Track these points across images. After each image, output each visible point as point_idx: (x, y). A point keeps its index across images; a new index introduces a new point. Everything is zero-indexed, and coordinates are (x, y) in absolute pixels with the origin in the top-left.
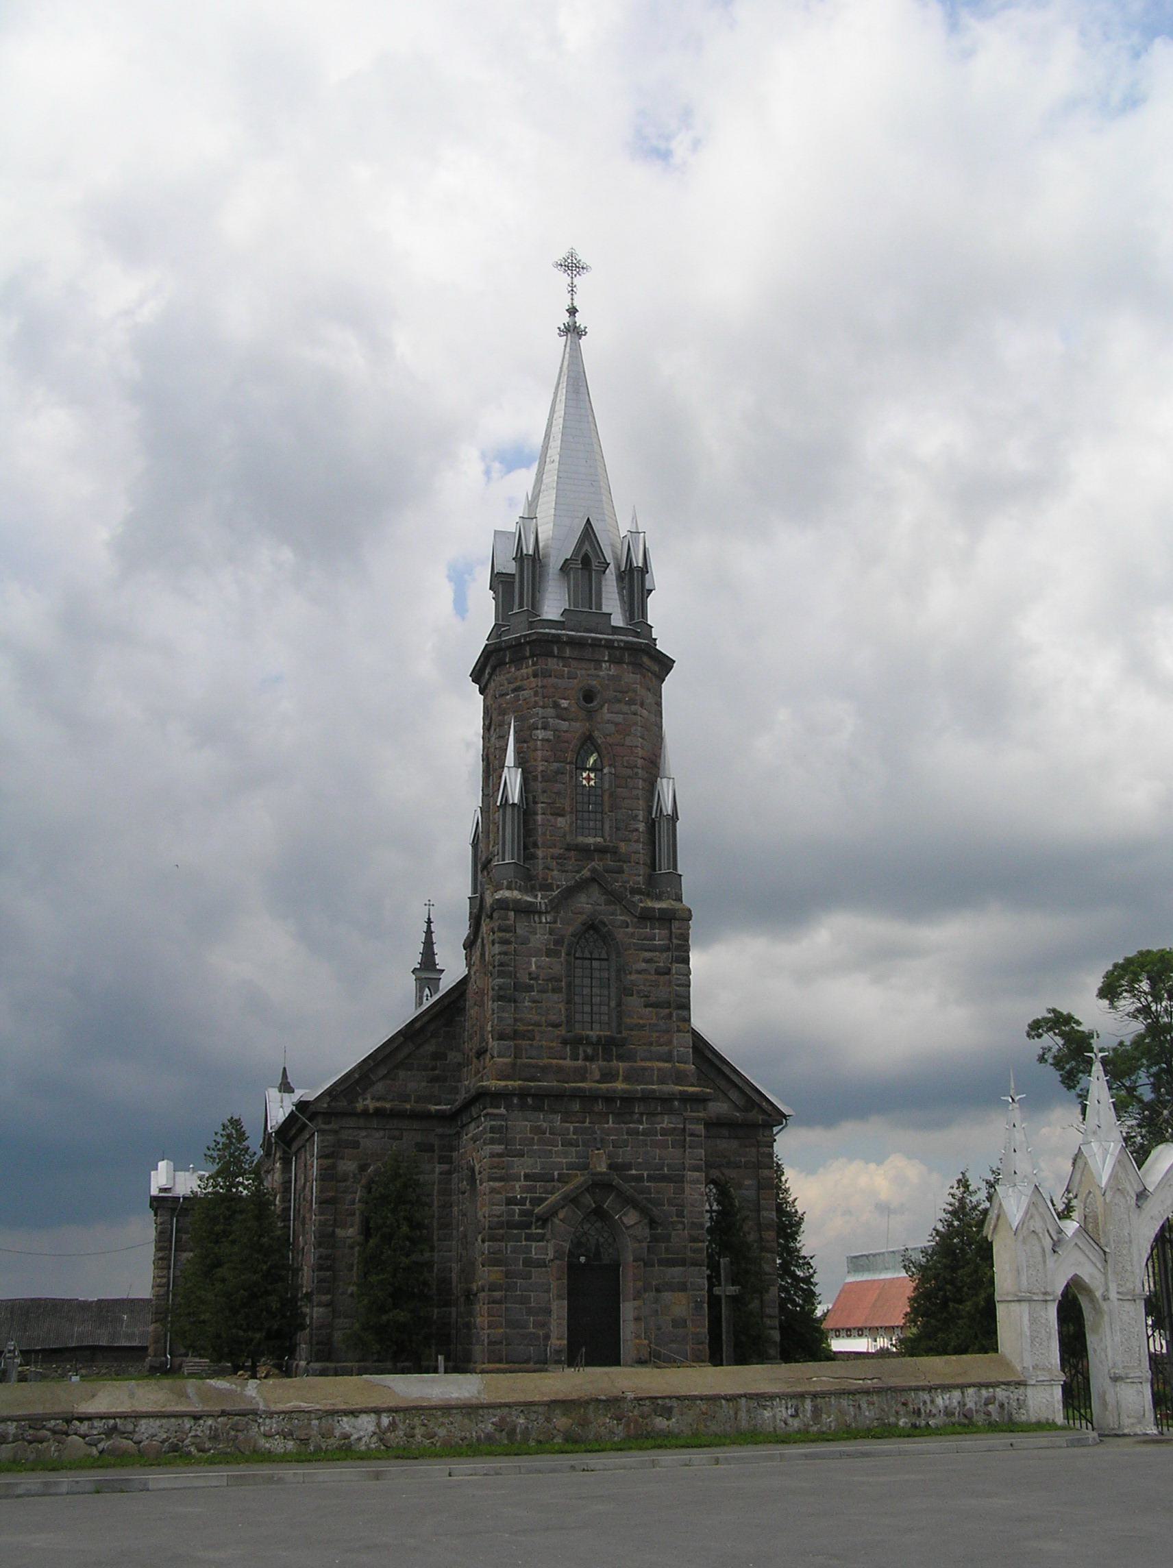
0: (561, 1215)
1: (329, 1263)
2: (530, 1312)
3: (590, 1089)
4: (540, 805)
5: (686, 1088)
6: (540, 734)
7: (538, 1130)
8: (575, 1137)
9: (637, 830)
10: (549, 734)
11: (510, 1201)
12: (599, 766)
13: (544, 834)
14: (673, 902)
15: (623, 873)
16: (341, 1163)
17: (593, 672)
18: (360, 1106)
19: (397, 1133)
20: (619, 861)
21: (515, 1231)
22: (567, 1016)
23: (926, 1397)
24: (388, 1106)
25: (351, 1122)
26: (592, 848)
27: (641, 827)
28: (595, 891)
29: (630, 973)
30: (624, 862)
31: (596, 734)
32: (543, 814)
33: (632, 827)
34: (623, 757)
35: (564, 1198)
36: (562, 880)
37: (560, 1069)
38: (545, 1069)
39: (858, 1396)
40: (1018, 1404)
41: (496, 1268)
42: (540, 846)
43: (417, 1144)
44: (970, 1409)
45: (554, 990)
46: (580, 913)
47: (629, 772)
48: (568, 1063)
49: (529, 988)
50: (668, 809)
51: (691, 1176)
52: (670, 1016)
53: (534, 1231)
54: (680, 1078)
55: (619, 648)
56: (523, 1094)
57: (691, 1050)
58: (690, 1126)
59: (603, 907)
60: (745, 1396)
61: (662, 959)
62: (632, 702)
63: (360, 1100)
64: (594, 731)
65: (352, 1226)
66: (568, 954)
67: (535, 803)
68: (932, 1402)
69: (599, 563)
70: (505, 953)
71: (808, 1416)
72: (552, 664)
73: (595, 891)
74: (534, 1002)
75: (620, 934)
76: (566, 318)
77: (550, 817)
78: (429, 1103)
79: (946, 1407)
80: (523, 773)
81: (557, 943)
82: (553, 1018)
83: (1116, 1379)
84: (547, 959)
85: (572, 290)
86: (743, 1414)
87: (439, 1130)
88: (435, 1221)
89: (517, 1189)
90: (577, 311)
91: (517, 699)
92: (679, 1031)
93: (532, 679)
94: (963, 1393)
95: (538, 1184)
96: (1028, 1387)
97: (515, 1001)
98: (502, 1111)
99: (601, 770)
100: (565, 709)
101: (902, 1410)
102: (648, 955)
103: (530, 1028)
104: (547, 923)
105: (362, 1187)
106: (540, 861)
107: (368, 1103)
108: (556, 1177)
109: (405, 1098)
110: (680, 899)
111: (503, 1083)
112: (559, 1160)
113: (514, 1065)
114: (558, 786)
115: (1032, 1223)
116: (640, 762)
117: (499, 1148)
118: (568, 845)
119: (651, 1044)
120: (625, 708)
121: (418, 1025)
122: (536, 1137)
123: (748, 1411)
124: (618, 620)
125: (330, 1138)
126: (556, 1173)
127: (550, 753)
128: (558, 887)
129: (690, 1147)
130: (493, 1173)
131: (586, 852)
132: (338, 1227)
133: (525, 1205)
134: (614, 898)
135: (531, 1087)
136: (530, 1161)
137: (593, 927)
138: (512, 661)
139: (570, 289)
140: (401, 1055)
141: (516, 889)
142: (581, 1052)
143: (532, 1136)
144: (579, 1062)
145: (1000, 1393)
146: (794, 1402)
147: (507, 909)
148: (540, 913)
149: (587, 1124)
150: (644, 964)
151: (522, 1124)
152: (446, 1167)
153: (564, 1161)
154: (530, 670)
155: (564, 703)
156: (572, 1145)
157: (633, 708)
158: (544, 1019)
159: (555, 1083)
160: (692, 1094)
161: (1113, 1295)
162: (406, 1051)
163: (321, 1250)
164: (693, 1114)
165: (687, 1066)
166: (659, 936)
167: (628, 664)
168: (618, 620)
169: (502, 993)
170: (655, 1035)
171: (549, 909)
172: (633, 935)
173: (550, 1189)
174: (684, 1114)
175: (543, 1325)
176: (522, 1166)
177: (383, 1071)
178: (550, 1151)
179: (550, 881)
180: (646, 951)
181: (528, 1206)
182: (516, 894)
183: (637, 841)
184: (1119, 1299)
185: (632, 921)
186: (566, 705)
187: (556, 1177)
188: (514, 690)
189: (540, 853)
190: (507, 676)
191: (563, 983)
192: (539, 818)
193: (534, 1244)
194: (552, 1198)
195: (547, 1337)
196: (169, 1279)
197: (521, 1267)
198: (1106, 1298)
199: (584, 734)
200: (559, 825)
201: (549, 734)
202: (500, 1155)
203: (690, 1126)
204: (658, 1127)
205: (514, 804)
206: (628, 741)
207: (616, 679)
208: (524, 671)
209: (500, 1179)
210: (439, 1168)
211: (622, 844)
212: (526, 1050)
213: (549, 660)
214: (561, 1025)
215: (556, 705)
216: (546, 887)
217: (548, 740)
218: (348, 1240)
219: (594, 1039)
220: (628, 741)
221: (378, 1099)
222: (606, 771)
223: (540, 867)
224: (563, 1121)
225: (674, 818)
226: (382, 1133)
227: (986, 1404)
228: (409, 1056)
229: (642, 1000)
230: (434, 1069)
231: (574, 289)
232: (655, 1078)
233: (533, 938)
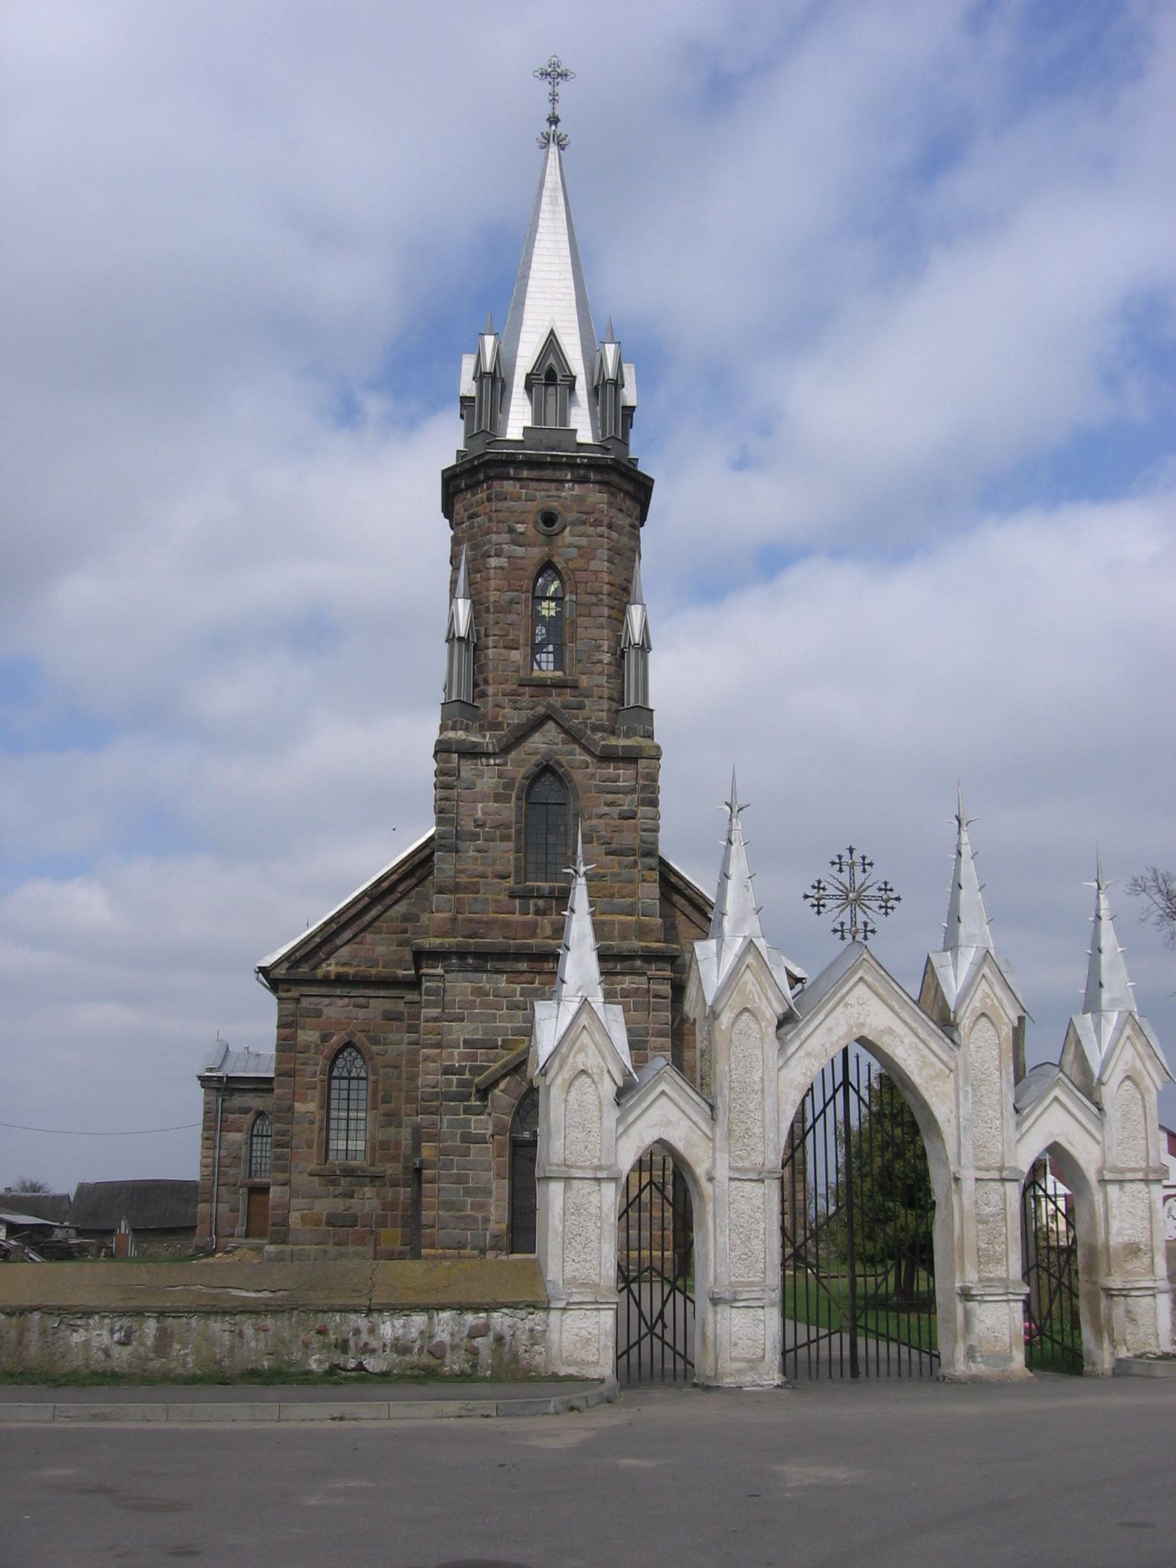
0: (502, 1085)
1: (287, 1138)
2: (468, 1192)
3: (537, 946)
4: (491, 638)
5: (649, 944)
6: (493, 562)
7: (479, 992)
8: (522, 999)
9: (600, 662)
10: (503, 561)
11: (448, 1071)
12: (560, 595)
13: (495, 668)
14: (638, 738)
15: (584, 709)
16: (300, 1032)
17: (554, 493)
18: (320, 973)
19: (363, 1001)
20: (580, 695)
21: (452, 1104)
22: (516, 867)
23: (361, 1321)
24: (351, 971)
25: (314, 990)
26: (549, 682)
27: (606, 658)
28: (551, 725)
29: (590, 818)
30: (586, 697)
31: (555, 559)
32: (494, 647)
33: (597, 657)
34: (586, 583)
35: (503, 1066)
36: (513, 717)
37: (506, 924)
38: (490, 924)
39: (238, 1318)
40: (531, 1337)
41: (429, 1144)
42: (490, 682)
44: (441, 1344)
45: (502, 839)
46: (534, 754)
47: (594, 599)
48: (517, 917)
49: (475, 837)
50: (637, 637)
51: (654, 1042)
52: (635, 864)
53: (474, 1103)
54: (643, 932)
55: (581, 466)
56: (462, 955)
57: (658, 902)
58: (654, 987)
59: (560, 746)
60: (38, 1309)
61: (628, 802)
62: (597, 523)
63: (324, 965)
64: (552, 556)
65: (313, 1100)
66: (518, 799)
67: (487, 636)
68: (372, 1330)
69: (563, 376)
70: (446, 799)
71: (149, 1343)
72: (509, 486)
73: (551, 725)
74: (479, 851)
75: (578, 776)
76: (545, 127)
77: (501, 650)
78: (399, 968)
79: (397, 1339)
80: (473, 603)
81: (508, 786)
82: (499, 868)
83: (715, 1302)
84: (496, 805)
85: (554, 99)
86: (33, 1336)
88: (403, 1094)
89: (455, 1057)
90: (559, 120)
91: (472, 527)
92: (643, 881)
93: (487, 504)
94: (431, 1318)
95: (479, 1051)
96: (552, 1313)
97: (457, 851)
98: (440, 971)
99: (562, 599)
100: (522, 533)
101: (316, 1340)
102: (610, 797)
103: (476, 879)
104: (495, 765)
106: (490, 698)
107: (331, 968)
108: (500, 1043)
109: (374, 963)
110: (650, 735)
111: (438, 941)
112: (504, 1024)
113: (454, 920)
114: (511, 618)
115: (580, 1058)
116: (606, 588)
117: (433, 1012)
118: (522, 680)
119: (612, 896)
120: (591, 530)
121: (385, 884)
122: (478, 1000)
123: (43, 1332)
124: (585, 435)
125: (292, 1006)
126: (500, 1039)
127: (503, 582)
128: (509, 725)
129: (654, 1010)
130: (428, 1039)
131: (542, 686)
132: (298, 1102)
133: (464, 1075)
134: (573, 736)
135: (469, 945)
136: (471, 1026)
137: (547, 769)
138: (468, 488)
139: (551, 98)
140: (368, 918)
141: (461, 729)
142: (531, 906)
143: (473, 998)
144: (530, 916)
145: (500, 1320)
146: (126, 1322)
147: (450, 752)
148: (488, 755)
149: (536, 985)
150: (606, 808)
151: (460, 985)
153: (509, 1025)
154: (484, 495)
155: (520, 528)
156: (518, 1008)
157: (599, 530)
158: (490, 869)
159: (501, 940)
160: (657, 950)
161: (722, 1173)
162: (373, 913)
164: (659, 973)
165: (653, 919)
166: (625, 775)
167: (595, 482)
168: (585, 435)
169: (443, 842)
170: (617, 885)
171: (497, 750)
172: (593, 775)
173: (492, 1057)
174: (649, 973)
175: (482, 1207)
176: (460, 1031)
177: (347, 934)
178: (494, 1015)
179: (500, 719)
180: (608, 793)
181: (467, 1076)
182: (461, 734)
183: (601, 673)
184: (731, 1179)
185: (593, 762)
186: (522, 530)
187: (500, 1043)
188: (470, 517)
189: (490, 690)
190: (464, 503)
191: (513, 830)
192: (490, 651)
193: (473, 1118)
194: (495, 1066)
195: (487, 1220)
197: (458, 1143)
198: (711, 1179)
199: (543, 559)
200: (513, 659)
201: (503, 561)
202: (435, 1019)
203: (654, 987)
204: (619, 987)
205: (460, 639)
206: (594, 565)
207: (581, 499)
208: (479, 496)
209: (438, 1045)
210: (408, 1037)
211: (584, 677)
212: (469, 904)
213: (505, 482)
214: (510, 877)
215: (511, 530)
216: (497, 726)
217: (501, 568)
219: (546, 892)
220: (594, 565)
221: (344, 965)
222: (567, 598)
223: (490, 705)
224: (509, 982)
225: (644, 648)
226: (346, 1000)
227: (472, 1336)
229: (604, 846)
230: (405, 931)
231: (557, 98)
232: (616, 933)
233: (479, 782)
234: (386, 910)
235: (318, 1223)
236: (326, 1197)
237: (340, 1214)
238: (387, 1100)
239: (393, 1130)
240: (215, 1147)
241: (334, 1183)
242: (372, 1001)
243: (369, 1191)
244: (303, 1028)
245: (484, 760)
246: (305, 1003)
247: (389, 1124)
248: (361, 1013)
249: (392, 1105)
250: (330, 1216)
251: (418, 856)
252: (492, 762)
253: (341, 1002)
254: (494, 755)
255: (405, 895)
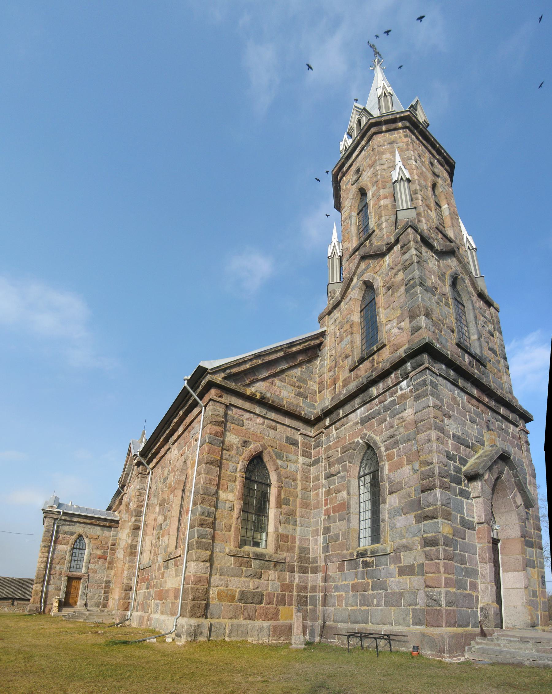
19: (274, 424)
43: (287, 437)
65: (232, 491)
87: (303, 431)
105: (244, 459)
152: (307, 460)
163: (203, 506)
177: (265, 374)
196: (48, 559)
210: (301, 460)
218: (228, 502)
235: (232, 599)
236: (240, 576)
237: (250, 592)
238: (287, 503)
239: (290, 527)
240: (49, 552)
241: (248, 564)
242: (279, 426)
243: (272, 574)
244: (229, 432)
246: (233, 412)
247: (287, 521)
248: (272, 433)
249: (291, 507)
250: (242, 593)
253: (260, 420)
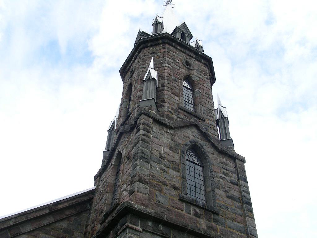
61: (234, 177)
72: (172, 48)
121: (61, 206)
177: (29, 228)
228: (49, 225)
234: (56, 222)
245: (165, 128)
251: (82, 199)
252: (169, 131)
254: (171, 128)
255: (68, 218)
